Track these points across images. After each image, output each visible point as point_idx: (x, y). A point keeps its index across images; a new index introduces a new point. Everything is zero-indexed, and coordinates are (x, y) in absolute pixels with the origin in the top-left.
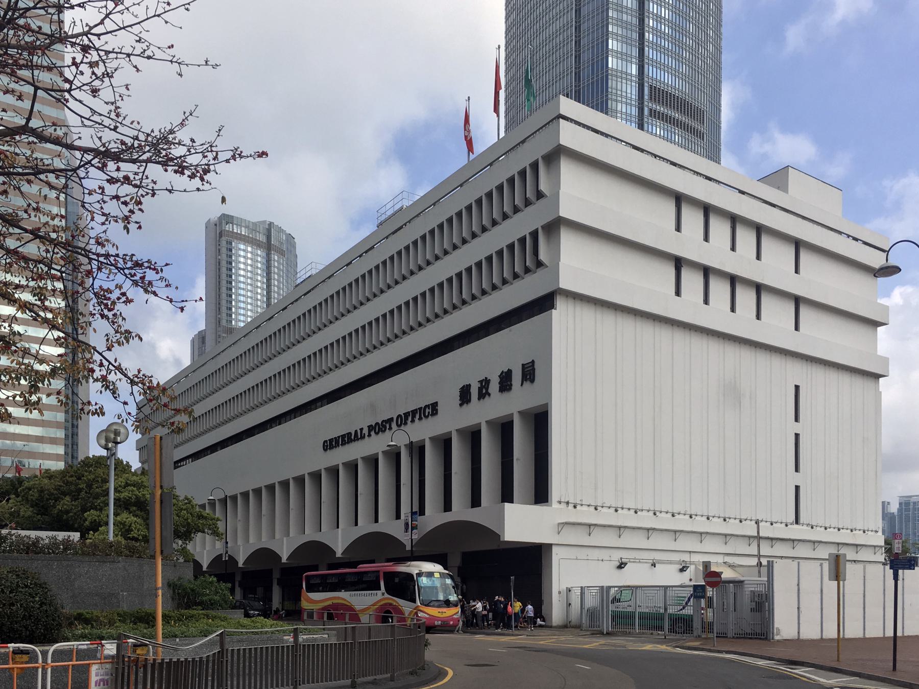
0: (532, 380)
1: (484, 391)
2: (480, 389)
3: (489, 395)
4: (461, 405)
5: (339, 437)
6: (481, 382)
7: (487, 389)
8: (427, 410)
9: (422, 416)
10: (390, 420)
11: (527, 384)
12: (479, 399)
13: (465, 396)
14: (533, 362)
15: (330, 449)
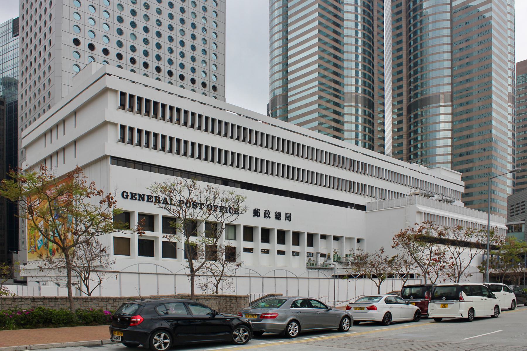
0: (290, 221)
1: (267, 215)
2: (265, 214)
3: (270, 218)
4: (254, 216)
5: (144, 195)
6: (266, 211)
7: (269, 215)
8: (231, 211)
9: (228, 211)
10: (202, 204)
11: (287, 221)
12: (265, 217)
13: (256, 213)
14: (290, 214)
15: (132, 198)
